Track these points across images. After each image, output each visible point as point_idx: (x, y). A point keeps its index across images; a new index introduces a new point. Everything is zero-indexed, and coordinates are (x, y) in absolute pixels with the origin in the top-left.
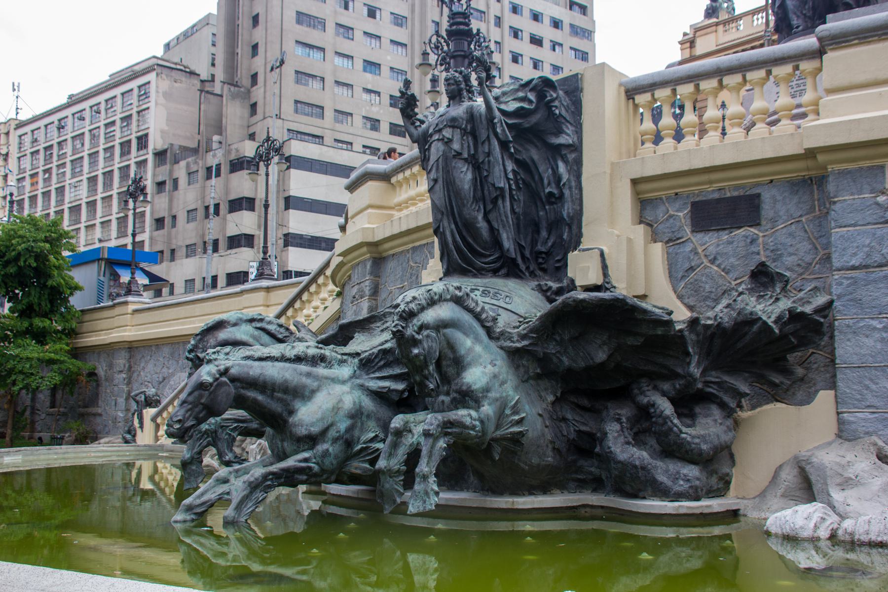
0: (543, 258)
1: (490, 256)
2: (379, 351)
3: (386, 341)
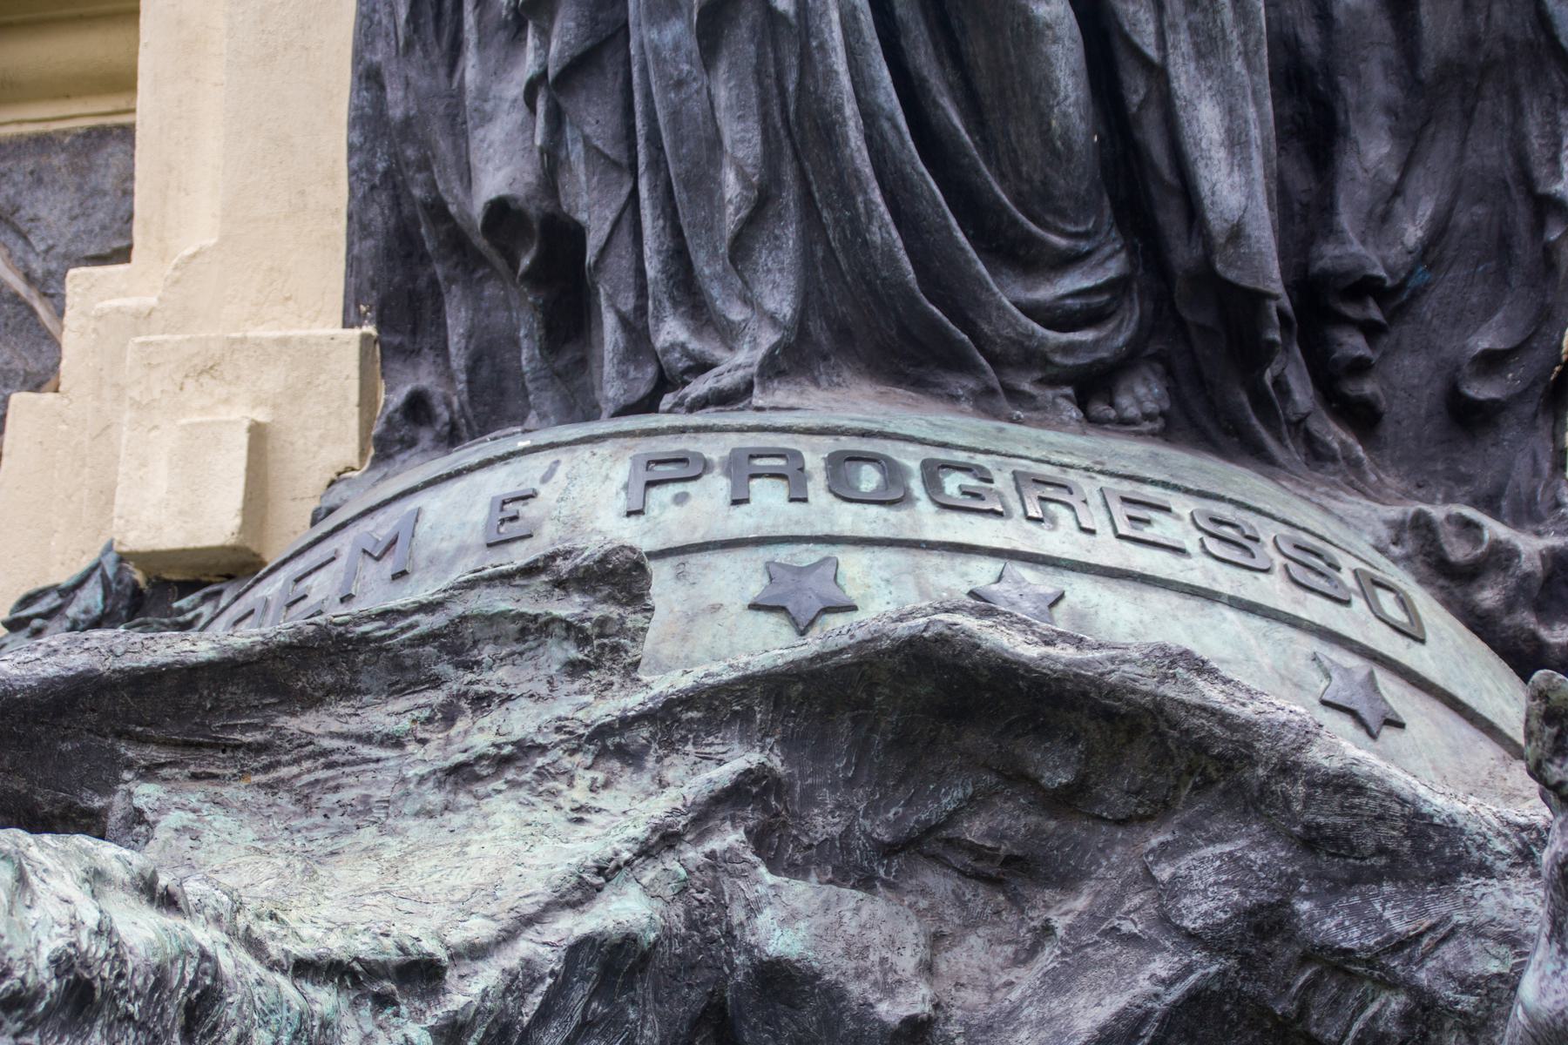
0: (1371, 331)
1: (1067, 262)
2: (580, 949)
3: (607, 871)
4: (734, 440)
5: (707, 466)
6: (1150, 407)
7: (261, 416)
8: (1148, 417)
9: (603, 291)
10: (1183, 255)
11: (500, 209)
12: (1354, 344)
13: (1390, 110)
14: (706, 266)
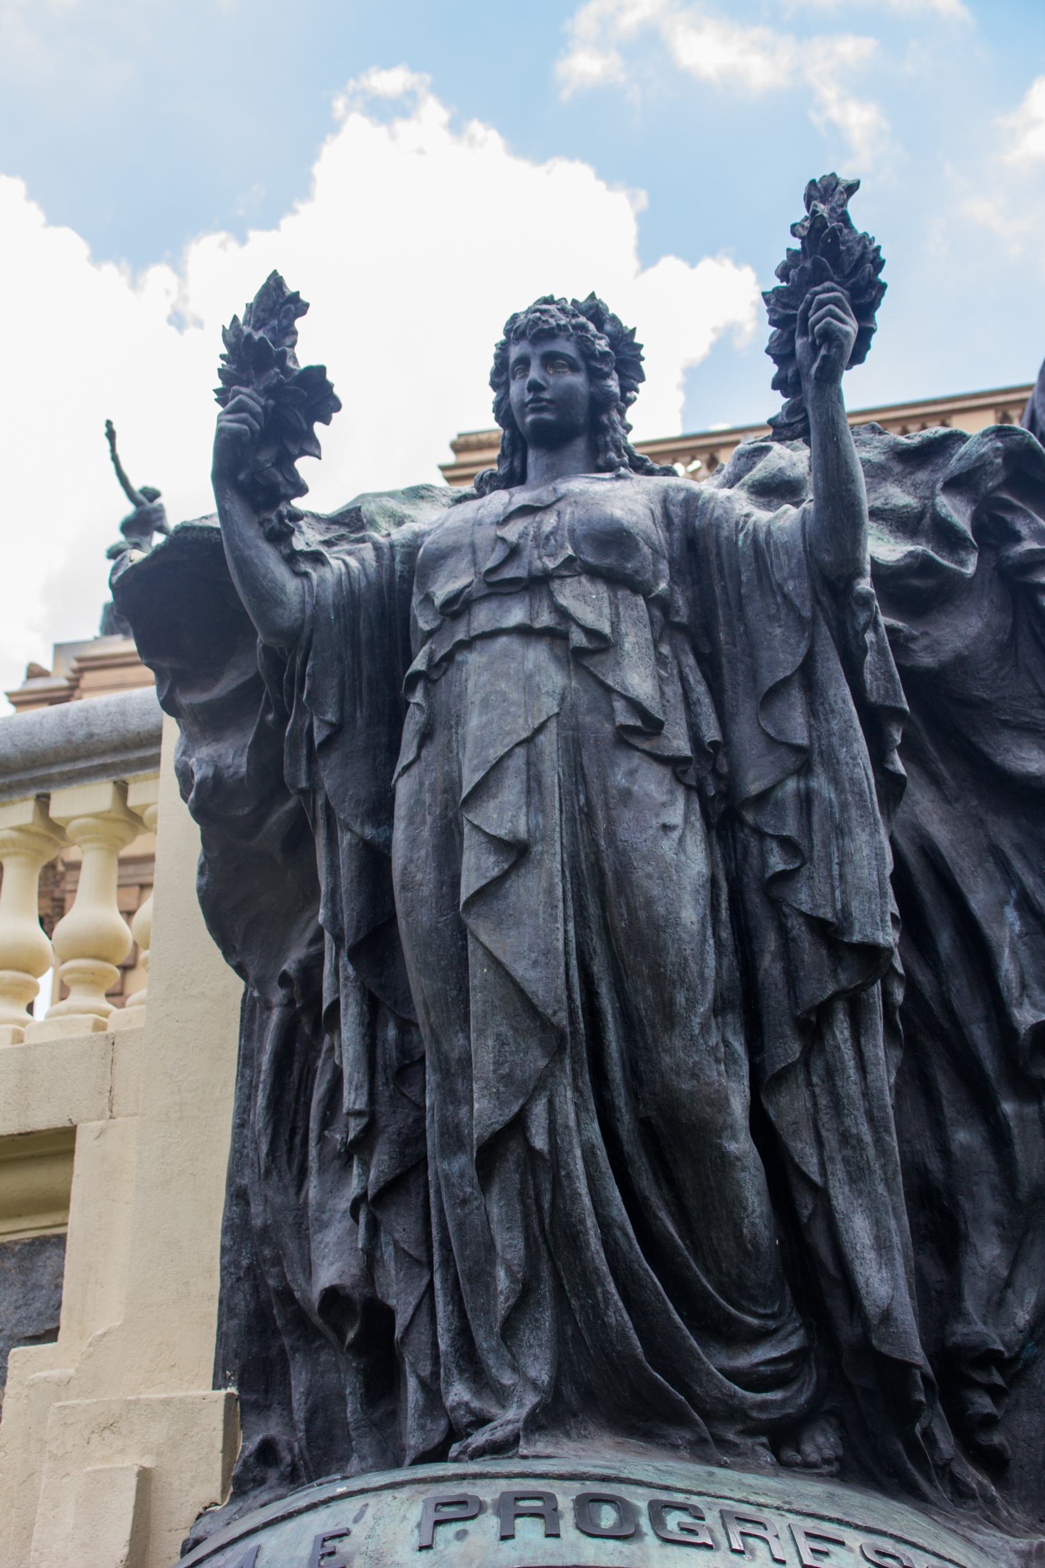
0: (996, 1393)
1: (759, 1337)
4: (503, 1485)
5: (482, 1507)
6: (828, 1453)
7: (148, 1462)
8: (827, 1461)
9: (408, 1359)
10: (847, 1332)
11: (332, 1294)
12: (984, 1404)
13: (998, 1222)
14: (485, 1341)
